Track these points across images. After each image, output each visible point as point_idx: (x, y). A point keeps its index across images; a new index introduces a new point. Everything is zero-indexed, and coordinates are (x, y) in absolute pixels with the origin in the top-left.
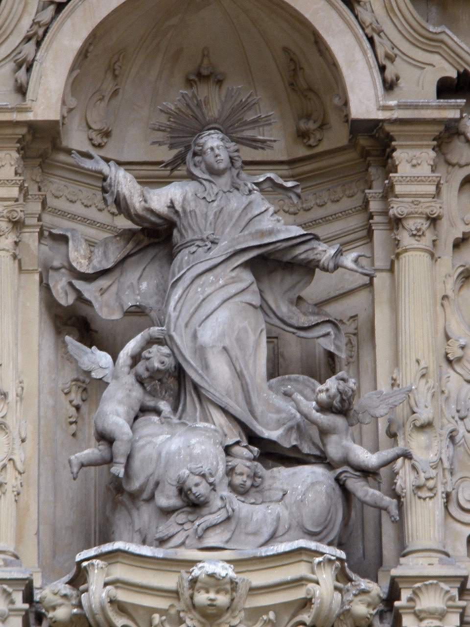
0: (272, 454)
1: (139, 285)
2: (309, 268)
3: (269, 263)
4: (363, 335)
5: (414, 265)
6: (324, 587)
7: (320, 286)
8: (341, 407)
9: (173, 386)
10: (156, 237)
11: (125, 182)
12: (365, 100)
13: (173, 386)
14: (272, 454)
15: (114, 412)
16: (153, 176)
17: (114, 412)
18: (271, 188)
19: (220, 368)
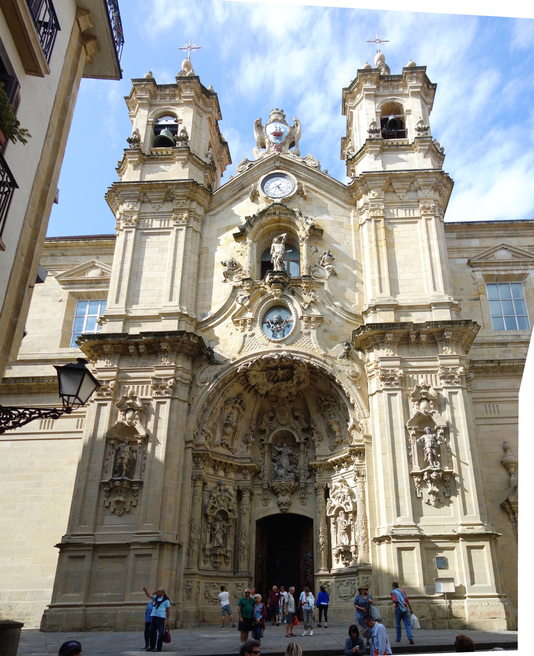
0: (289, 472)
1: (278, 457)
2: (293, 455)
3: (290, 455)
4: (298, 461)
5: (302, 455)
6: (293, 484)
7: (294, 457)
8: (295, 468)
9: (280, 466)
10: (280, 453)
11: (277, 448)
12: (298, 440)
13: (280, 466)
14: (289, 472)
15: (276, 469)
16: (279, 447)
17: (276, 469)
18: (290, 448)
19: (285, 465)
